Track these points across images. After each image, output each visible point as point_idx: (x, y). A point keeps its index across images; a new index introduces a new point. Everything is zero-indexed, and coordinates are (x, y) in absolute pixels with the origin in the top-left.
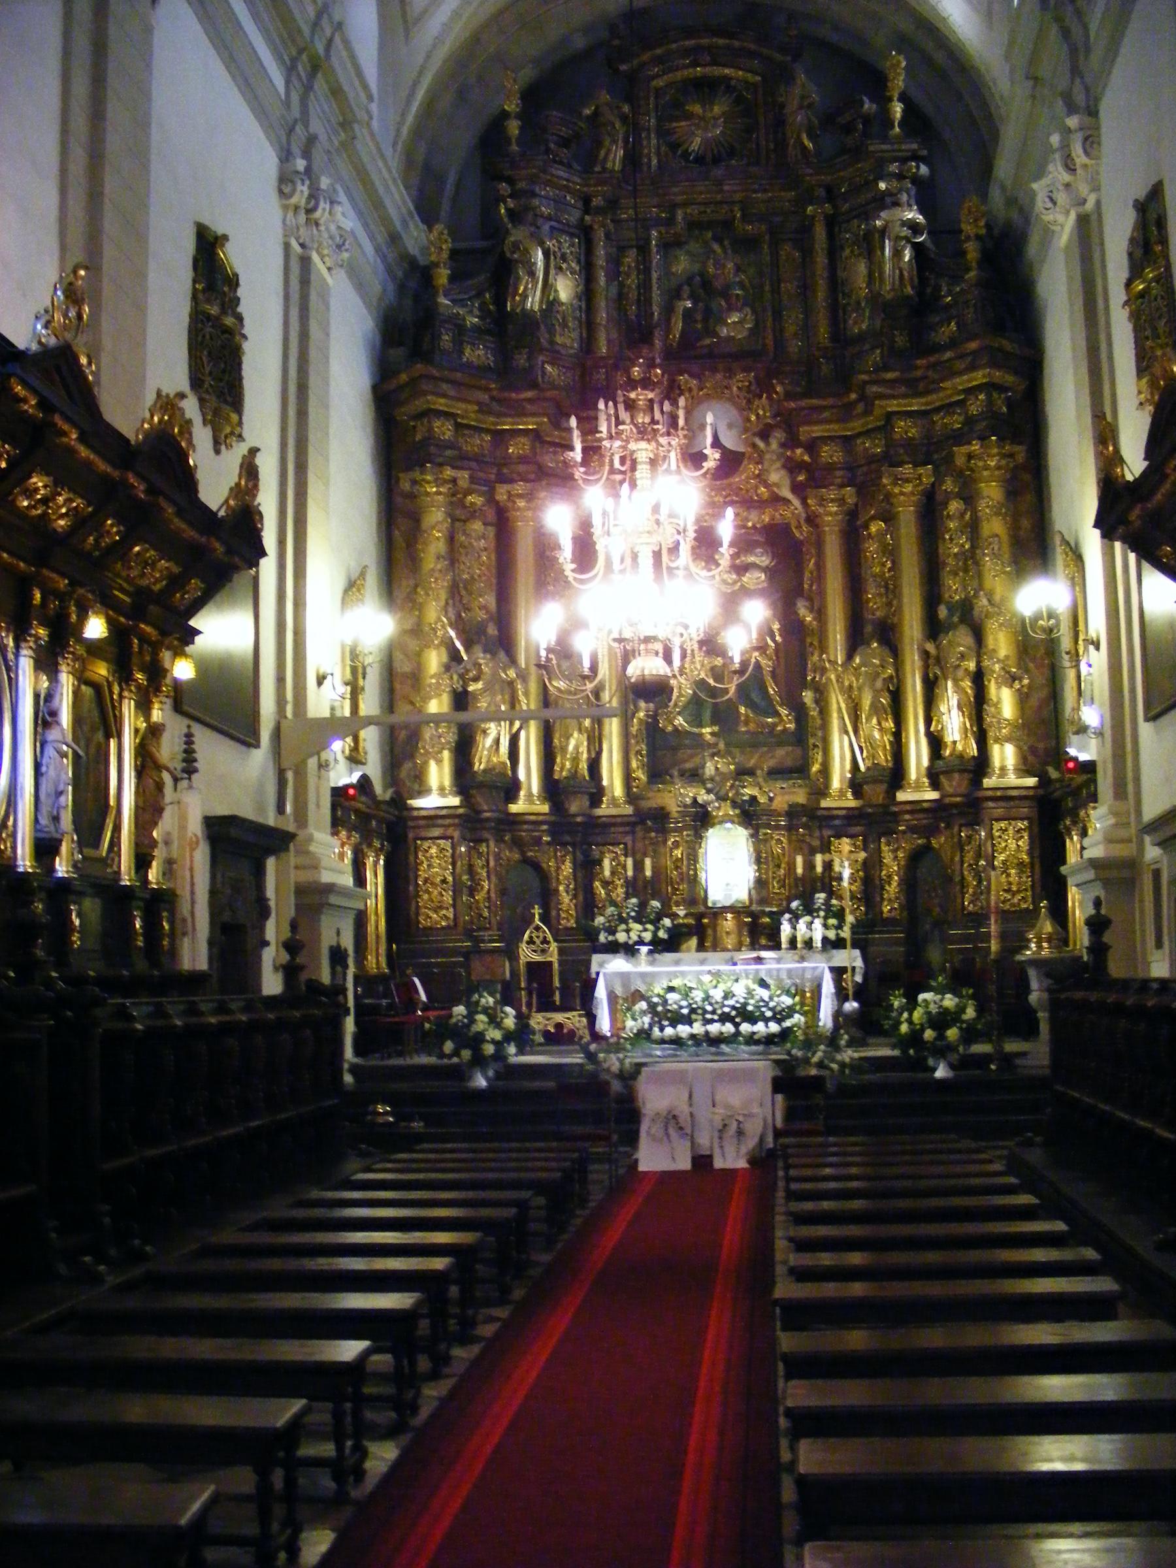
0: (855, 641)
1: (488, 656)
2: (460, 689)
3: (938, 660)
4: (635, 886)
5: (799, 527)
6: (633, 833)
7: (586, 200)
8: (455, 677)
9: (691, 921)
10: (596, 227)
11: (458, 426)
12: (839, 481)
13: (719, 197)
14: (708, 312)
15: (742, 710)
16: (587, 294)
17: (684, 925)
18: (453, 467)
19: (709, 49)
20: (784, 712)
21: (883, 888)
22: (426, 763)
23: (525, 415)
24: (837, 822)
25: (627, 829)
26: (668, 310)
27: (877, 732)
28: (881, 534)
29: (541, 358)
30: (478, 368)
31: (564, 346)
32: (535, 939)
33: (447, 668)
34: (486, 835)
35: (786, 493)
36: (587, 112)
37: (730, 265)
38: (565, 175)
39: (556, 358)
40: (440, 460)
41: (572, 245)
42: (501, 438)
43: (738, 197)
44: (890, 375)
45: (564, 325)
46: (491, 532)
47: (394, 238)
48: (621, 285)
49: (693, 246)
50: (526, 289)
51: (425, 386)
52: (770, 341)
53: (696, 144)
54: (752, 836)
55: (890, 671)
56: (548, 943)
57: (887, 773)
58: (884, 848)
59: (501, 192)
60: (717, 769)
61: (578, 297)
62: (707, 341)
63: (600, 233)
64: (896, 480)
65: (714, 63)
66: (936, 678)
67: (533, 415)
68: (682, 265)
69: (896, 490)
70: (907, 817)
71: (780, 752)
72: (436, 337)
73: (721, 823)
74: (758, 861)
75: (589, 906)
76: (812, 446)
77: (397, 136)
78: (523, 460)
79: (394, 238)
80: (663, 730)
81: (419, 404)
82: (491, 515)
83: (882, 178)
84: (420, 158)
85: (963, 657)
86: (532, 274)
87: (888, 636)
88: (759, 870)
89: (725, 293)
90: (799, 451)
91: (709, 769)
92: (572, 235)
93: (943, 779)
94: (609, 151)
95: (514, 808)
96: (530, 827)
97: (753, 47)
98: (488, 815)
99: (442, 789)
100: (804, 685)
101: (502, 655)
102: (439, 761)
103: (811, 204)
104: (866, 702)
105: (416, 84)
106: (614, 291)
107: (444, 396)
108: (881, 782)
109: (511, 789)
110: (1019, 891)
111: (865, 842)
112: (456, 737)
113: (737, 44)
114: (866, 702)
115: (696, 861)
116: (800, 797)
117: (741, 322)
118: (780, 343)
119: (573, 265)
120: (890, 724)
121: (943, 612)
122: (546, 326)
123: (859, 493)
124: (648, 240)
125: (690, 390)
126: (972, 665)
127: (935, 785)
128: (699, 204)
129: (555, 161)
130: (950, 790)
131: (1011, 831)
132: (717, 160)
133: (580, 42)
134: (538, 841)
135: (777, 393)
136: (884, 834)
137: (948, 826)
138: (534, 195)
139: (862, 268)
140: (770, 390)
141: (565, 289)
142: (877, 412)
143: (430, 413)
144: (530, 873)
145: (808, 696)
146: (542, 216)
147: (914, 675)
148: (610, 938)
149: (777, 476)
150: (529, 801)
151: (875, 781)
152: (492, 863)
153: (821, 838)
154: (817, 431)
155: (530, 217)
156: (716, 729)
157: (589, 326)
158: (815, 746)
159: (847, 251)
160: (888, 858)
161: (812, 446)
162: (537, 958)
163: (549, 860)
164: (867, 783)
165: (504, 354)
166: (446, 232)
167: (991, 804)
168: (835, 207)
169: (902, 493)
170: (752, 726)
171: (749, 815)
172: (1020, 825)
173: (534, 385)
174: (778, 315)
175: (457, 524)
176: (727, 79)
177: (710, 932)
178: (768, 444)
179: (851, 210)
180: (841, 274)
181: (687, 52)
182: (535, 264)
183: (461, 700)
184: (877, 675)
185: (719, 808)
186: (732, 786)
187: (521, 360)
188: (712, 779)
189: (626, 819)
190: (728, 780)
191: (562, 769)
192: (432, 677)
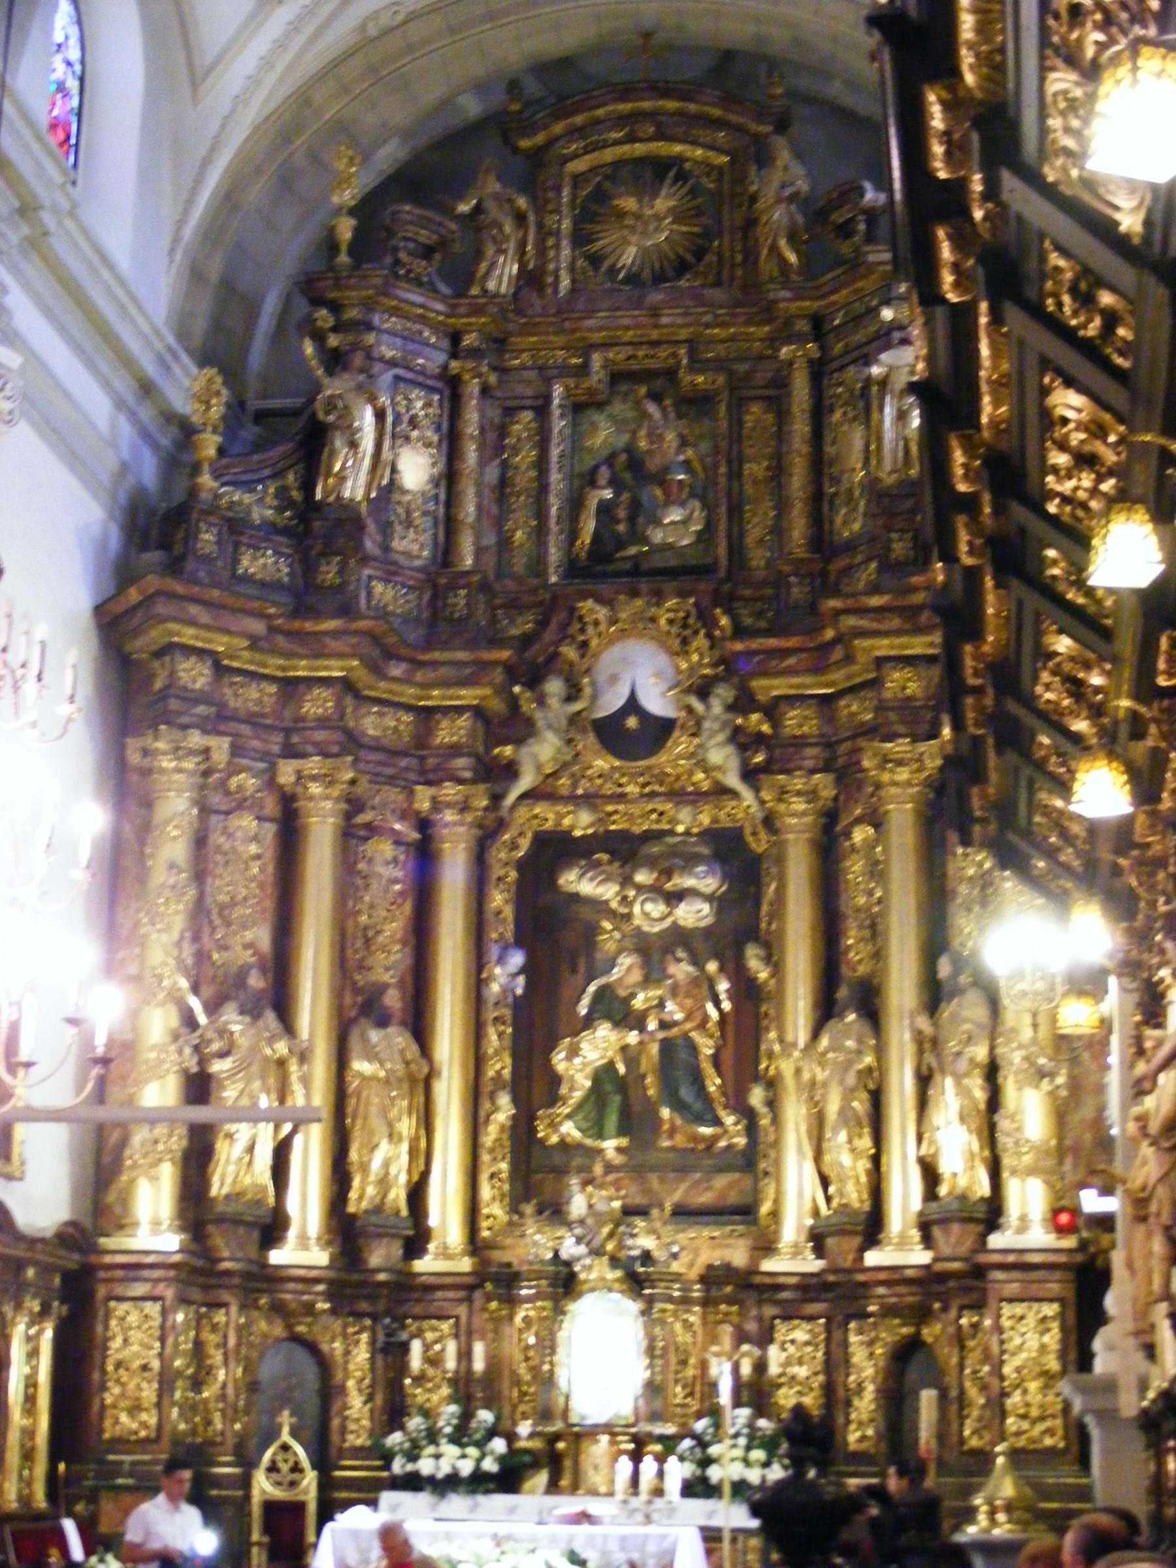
0: (826, 1010)
1: (248, 1019)
2: (195, 1069)
3: (935, 1042)
4: (466, 1390)
5: (754, 834)
6: (469, 1300)
7: (455, 338)
8: (187, 1051)
9: (537, 1444)
10: (467, 377)
11: (220, 670)
12: (809, 764)
13: (655, 335)
14: (635, 507)
15: (665, 1113)
16: (449, 478)
17: (526, 1451)
18: (205, 732)
19: (651, 115)
20: (729, 1120)
21: (848, 1404)
22: (132, 1181)
23: (330, 656)
24: (785, 1295)
25: (462, 1294)
26: (575, 505)
27: (848, 1156)
28: (870, 845)
29: (367, 572)
30: (263, 584)
31: (408, 554)
32: (281, 1465)
33: (176, 1037)
34: (225, 1296)
35: (732, 780)
36: (464, 208)
37: (671, 437)
38: (419, 299)
39: (391, 572)
40: (185, 720)
41: (427, 405)
42: (291, 687)
43: (684, 334)
44: (876, 601)
45: (408, 523)
46: (270, 830)
47: (147, 388)
48: (505, 465)
49: (619, 408)
50: (343, 467)
51: (161, 608)
52: (722, 550)
53: (629, 256)
54: (643, 1313)
55: (869, 1060)
56: (301, 1471)
57: (863, 1217)
58: (853, 1339)
59: (320, 323)
60: (590, 1206)
61: (435, 482)
62: (633, 550)
63: (473, 387)
64: (884, 759)
65: (660, 136)
66: (930, 1070)
67: (340, 656)
68: (603, 434)
69: (886, 777)
70: (881, 1290)
71: (721, 1181)
72: (192, 536)
73: (592, 1290)
74: (650, 1351)
75: (394, 1412)
76: (772, 710)
77: (176, 239)
78: (322, 723)
79: (147, 388)
80: (541, 1142)
81: (155, 636)
82: (271, 806)
83: (887, 302)
84: (214, 276)
85: (970, 1040)
86: (353, 445)
87: (871, 1005)
88: (651, 1366)
89: (661, 478)
90: (755, 717)
91: (578, 1205)
92: (432, 390)
93: (936, 1232)
94: (492, 266)
95: (276, 1257)
96: (300, 1287)
97: (716, 112)
98: (226, 1265)
99: (156, 1223)
100: (757, 1077)
101: (270, 1017)
102: (154, 1179)
103: (789, 343)
104: (833, 1107)
105: (206, 163)
106: (492, 473)
107: (192, 622)
108: (852, 1233)
110: (1042, 1418)
111: (828, 1328)
112: (184, 1143)
113: (692, 107)
114: (833, 1107)
115: (553, 1350)
116: (738, 1255)
117: (685, 522)
118: (736, 550)
119: (429, 434)
120: (865, 1143)
121: (944, 968)
122: (377, 522)
123: (839, 781)
124: (548, 399)
125: (596, 623)
126: (981, 1052)
127: (927, 1241)
128: (629, 343)
129: (409, 280)
130: (946, 1250)
131: (1031, 1320)
132: (659, 278)
133: (472, 107)
134: (309, 1309)
135: (722, 629)
136: (849, 1318)
137: (945, 1309)
138: (369, 327)
139: (857, 437)
140: (709, 623)
141: (415, 469)
142: (862, 658)
143: (166, 650)
144: (301, 1356)
145: (757, 1097)
146: (382, 359)
147: (902, 1064)
148: (410, 1467)
149: (722, 756)
151: (841, 1232)
152: (232, 1341)
153: (760, 1319)
154: (778, 687)
155: (358, 359)
156: (624, 1142)
157: (450, 525)
158: (766, 1174)
159: (837, 416)
160: (858, 1355)
161: (772, 710)
162: (278, 1494)
163: (333, 1340)
164: (832, 1234)
165: (307, 565)
166: (219, 380)
167: (999, 1275)
168: (822, 348)
169: (895, 784)
170: (680, 1140)
171: (637, 1279)
172: (1051, 1309)
173: (347, 610)
174: (735, 511)
175: (214, 819)
176: (680, 159)
177: (568, 1463)
178: (708, 707)
179: (846, 352)
180: (830, 450)
181: (621, 120)
182: (359, 429)
183: (199, 1087)
184: (848, 1065)
185: (589, 1268)
186: (611, 1235)
187: (329, 573)
188: (582, 1222)
189: (458, 1280)
190: (605, 1223)
191: (361, 1198)
192: (153, 1048)
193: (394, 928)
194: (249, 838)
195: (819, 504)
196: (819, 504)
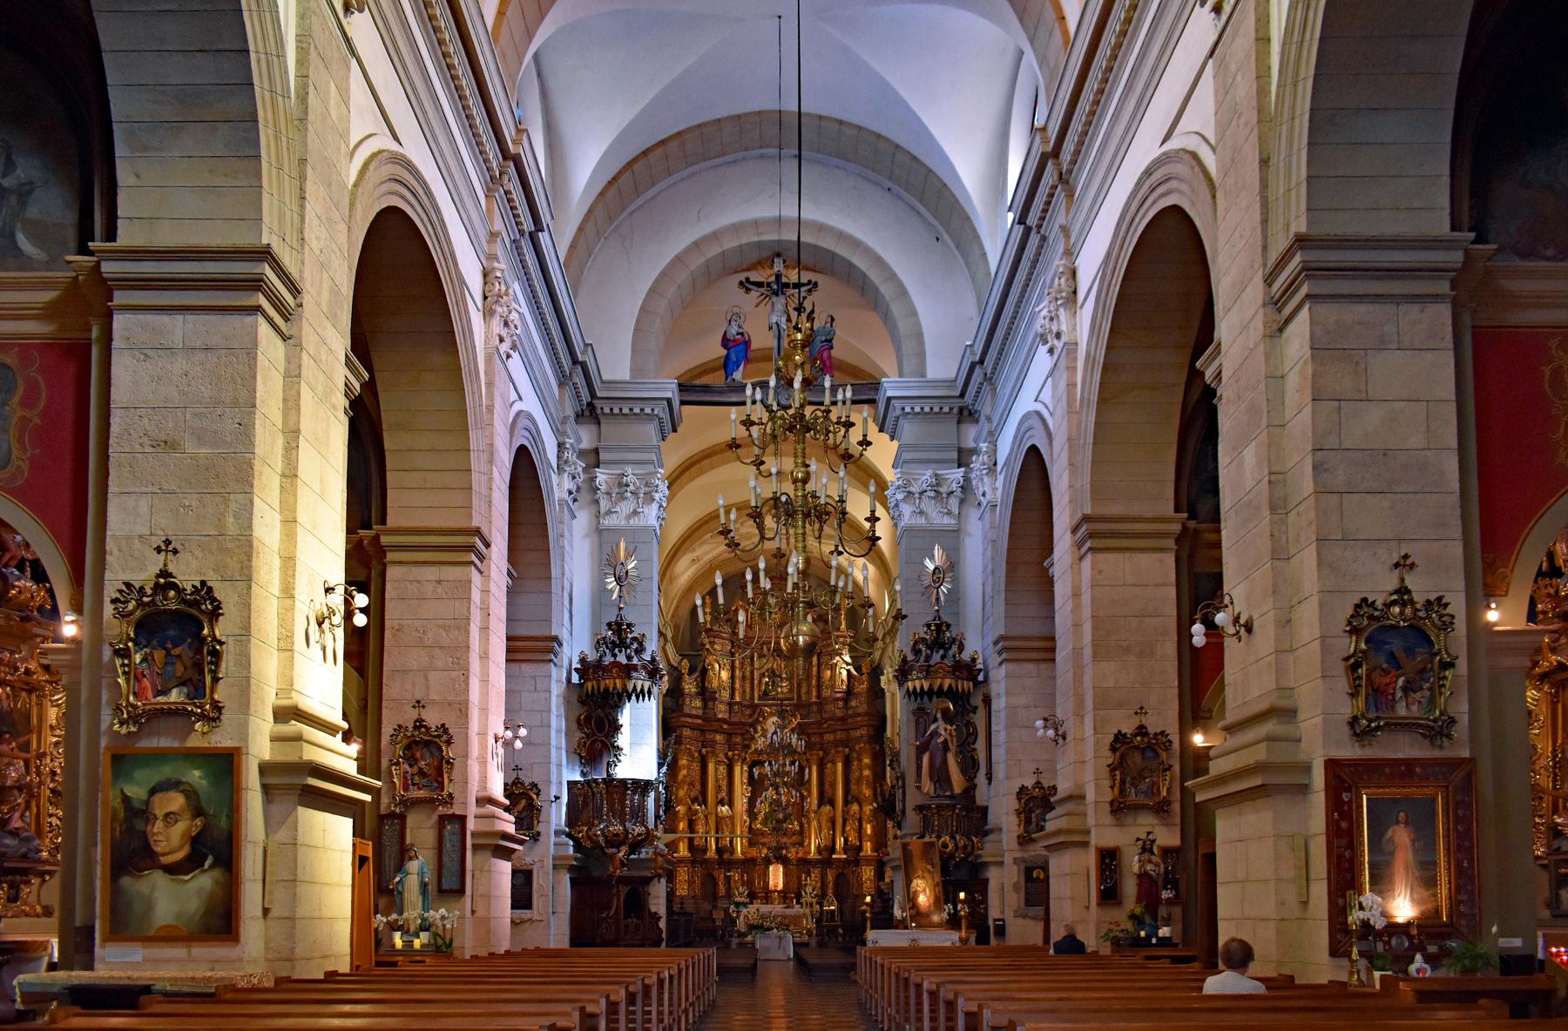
16: (732, 677)
87: (832, 803)
109: (705, 850)
141: (725, 675)
150: (712, 853)
157: (733, 689)
187: (710, 704)
193: (724, 784)
194: (696, 766)
195: (819, 687)
196: (819, 687)
